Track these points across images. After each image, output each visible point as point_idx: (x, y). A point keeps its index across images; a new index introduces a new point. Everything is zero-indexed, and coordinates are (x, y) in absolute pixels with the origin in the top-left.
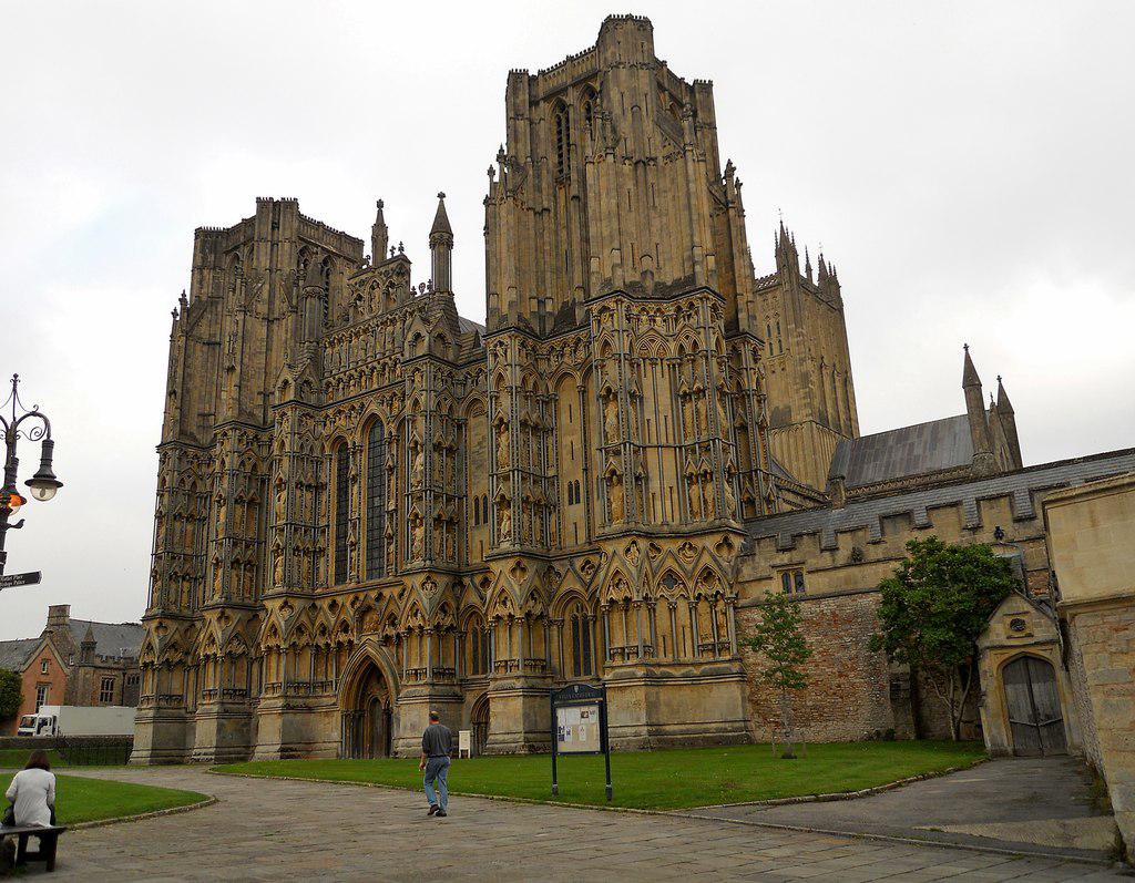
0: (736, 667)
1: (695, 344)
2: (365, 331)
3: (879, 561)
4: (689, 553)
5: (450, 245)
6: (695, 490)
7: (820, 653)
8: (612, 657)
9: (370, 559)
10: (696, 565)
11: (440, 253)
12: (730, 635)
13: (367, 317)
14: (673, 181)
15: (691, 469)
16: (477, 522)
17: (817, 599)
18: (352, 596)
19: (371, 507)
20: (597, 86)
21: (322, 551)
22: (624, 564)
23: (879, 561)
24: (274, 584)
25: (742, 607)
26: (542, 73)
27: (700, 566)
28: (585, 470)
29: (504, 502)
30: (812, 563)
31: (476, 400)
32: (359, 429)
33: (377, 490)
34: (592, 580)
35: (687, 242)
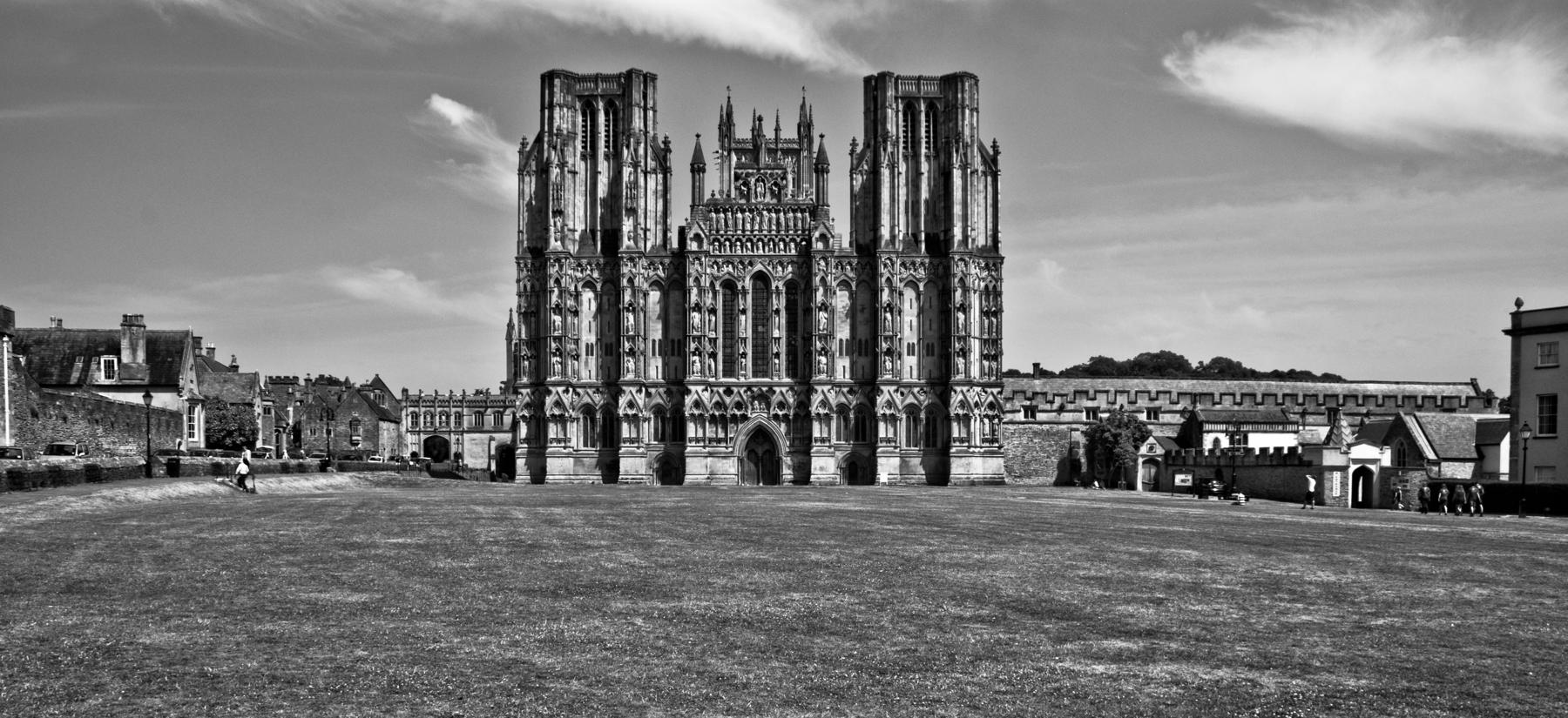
0: (1002, 450)
5: (827, 173)
6: (986, 363)
9: (754, 364)
12: (999, 435)
13: (753, 201)
15: (986, 352)
16: (841, 354)
17: (1041, 423)
18: (745, 388)
19: (755, 331)
21: (713, 355)
24: (693, 373)
27: (988, 401)
30: (1041, 407)
32: (748, 278)
33: (760, 322)
35: (990, 226)
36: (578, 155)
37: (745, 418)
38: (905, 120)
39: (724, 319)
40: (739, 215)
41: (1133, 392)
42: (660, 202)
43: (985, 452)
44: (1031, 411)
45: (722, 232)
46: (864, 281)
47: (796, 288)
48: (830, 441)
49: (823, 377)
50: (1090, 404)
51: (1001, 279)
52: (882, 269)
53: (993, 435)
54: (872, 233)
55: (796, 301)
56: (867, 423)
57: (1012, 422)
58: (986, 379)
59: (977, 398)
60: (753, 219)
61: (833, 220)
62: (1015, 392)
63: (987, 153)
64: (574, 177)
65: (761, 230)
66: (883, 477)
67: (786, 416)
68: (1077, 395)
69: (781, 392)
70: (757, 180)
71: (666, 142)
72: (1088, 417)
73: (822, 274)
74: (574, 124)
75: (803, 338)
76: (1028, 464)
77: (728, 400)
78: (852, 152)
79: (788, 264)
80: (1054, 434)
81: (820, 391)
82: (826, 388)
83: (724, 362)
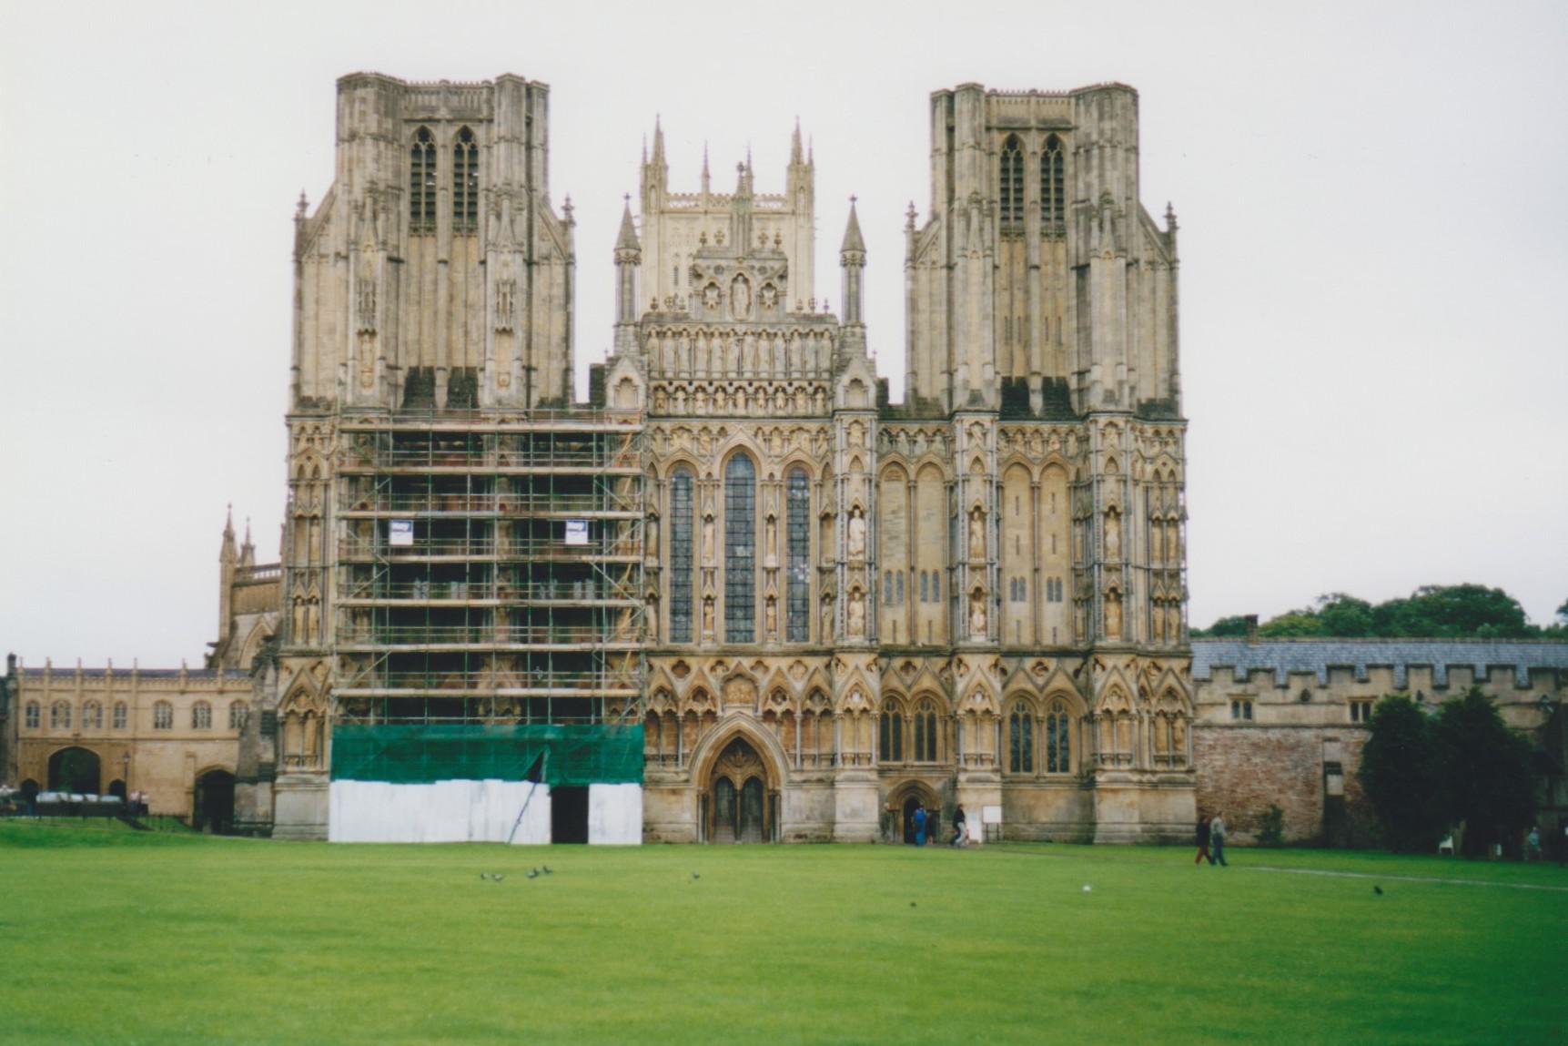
0: (1192, 779)
1: (1172, 473)
2: (721, 334)
3: (1322, 704)
4: (1154, 672)
5: (862, 265)
6: (1159, 613)
7: (1263, 772)
8: (1103, 761)
9: (730, 617)
10: (1161, 682)
11: (849, 273)
12: (1185, 749)
13: (729, 318)
14: (1154, 291)
15: (1158, 594)
17: (1266, 727)
18: (712, 661)
19: (731, 556)
20: (1068, 141)
22: (1124, 679)
23: (1322, 704)
25: (1195, 727)
26: (994, 93)
27: (1165, 685)
28: (1036, 570)
29: (977, 594)
30: (1264, 696)
31: (895, 463)
32: (719, 459)
34: (1047, 683)
35: (1163, 362)
36: (405, 228)
37: (710, 715)
38: (1005, 170)
39: (674, 533)
40: (702, 343)
41: (1440, 667)
42: (558, 318)
43: (1162, 782)
44: (1243, 706)
45: (669, 375)
46: (930, 464)
47: (805, 478)
48: (869, 760)
49: (857, 640)
50: (1358, 691)
51: (1183, 460)
52: (962, 442)
53: (1175, 749)
54: (945, 376)
55: (805, 501)
56: (939, 728)
57: (1209, 726)
58: (1158, 644)
59: (1143, 680)
60: (724, 350)
61: (875, 353)
62: (1215, 669)
63: (1155, 229)
64: (397, 270)
65: (740, 373)
66: (973, 829)
67: (788, 713)
68: (1335, 675)
69: (779, 671)
70: (735, 280)
71: (567, 209)
72: (1355, 715)
73: (855, 451)
74: (398, 174)
75: (821, 570)
76: (1242, 805)
77: (682, 687)
78: (911, 226)
79: (792, 432)
80: (1294, 748)
81: (851, 667)
82: (864, 659)
83: (674, 613)
